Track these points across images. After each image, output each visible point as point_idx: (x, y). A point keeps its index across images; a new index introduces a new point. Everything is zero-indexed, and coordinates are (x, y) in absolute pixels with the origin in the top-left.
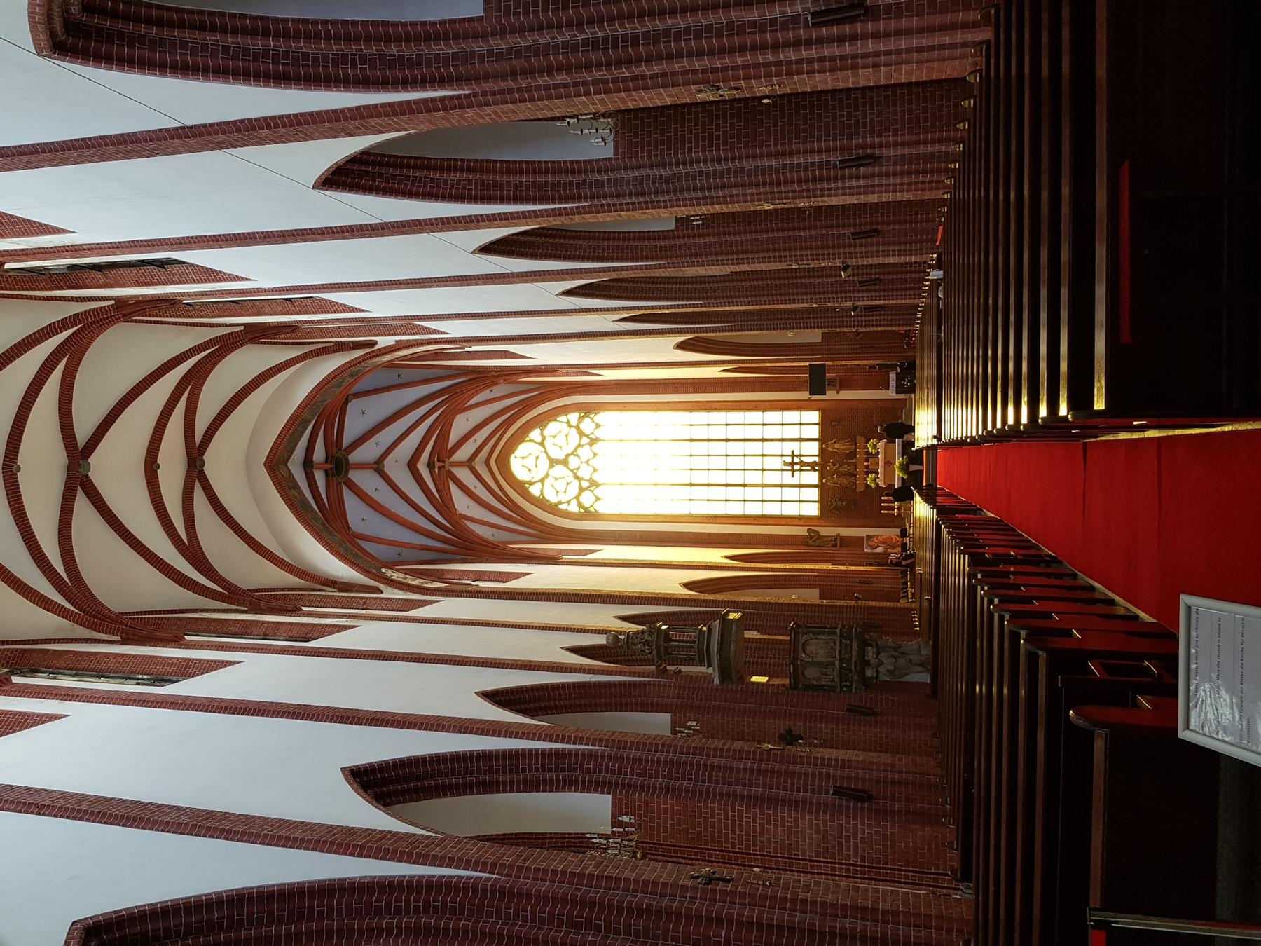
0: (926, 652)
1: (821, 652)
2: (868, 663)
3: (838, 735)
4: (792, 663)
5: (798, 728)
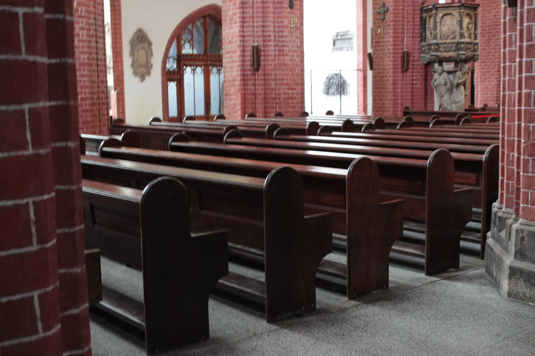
0: (453, 108)
1: (445, 29)
2: (440, 64)
3: (386, 46)
4: (433, 6)
5: (390, 16)
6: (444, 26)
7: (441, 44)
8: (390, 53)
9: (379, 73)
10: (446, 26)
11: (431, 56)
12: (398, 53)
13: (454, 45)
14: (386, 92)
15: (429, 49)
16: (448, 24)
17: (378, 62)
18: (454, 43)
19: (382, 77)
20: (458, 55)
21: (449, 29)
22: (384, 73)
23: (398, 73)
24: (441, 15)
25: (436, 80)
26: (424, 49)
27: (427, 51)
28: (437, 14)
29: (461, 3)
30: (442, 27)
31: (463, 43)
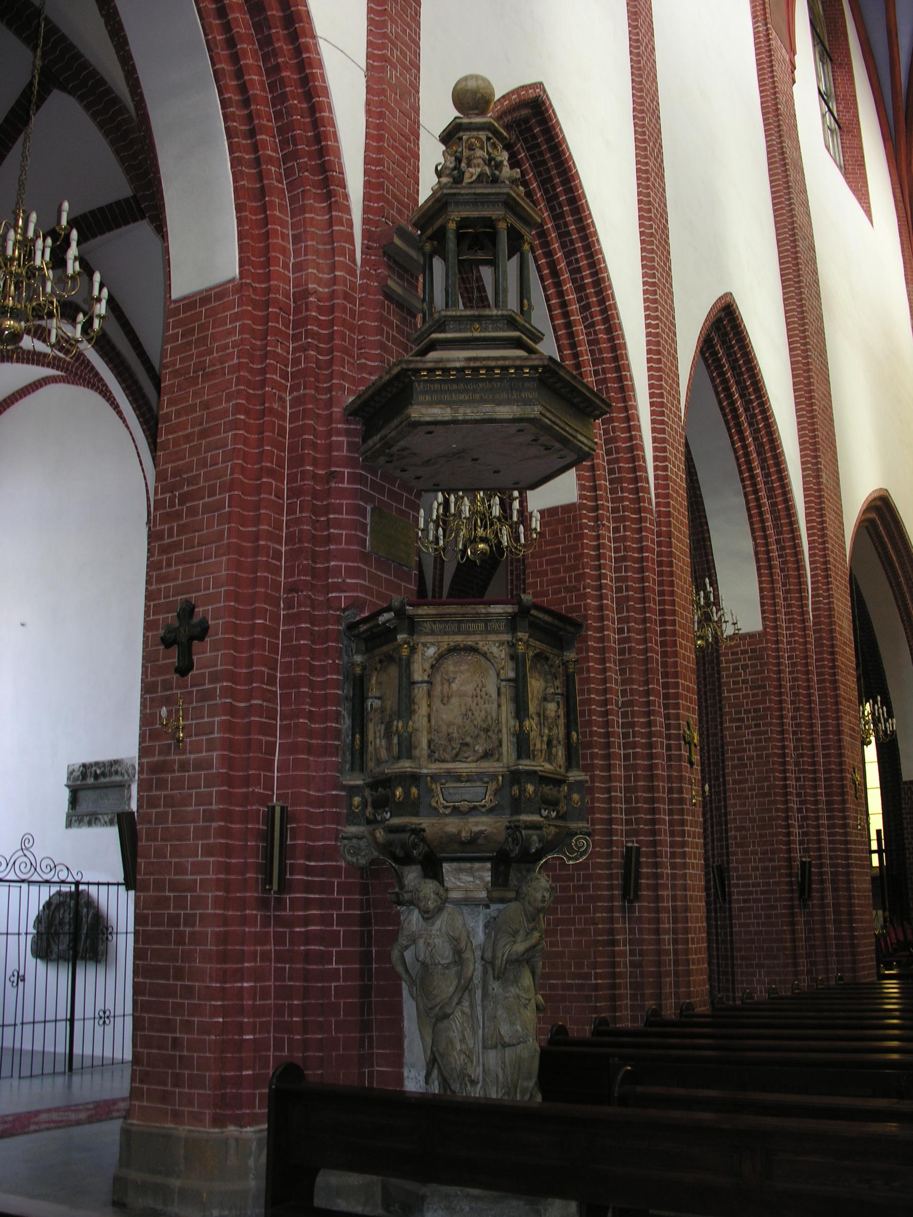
1: (450, 714)
5: (208, 656)
6: (445, 699)
7: (435, 777)
8: (209, 816)
9: (162, 902)
10: (455, 700)
11: (392, 830)
12: (245, 817)
13: (492, 787)
14: (188, 992)
15: (380, 804)
16: (462, 695)
17: (160, 853)
18: (493, 777)
19: (174, 920)
20: (513, 828)
21: (467, 714)
22: (180, 903)
23: (242, 904)
24: (431, 651)
25: (413, 940)
26: (357, 800)
27: (369, 809)
28: (413, 650)
29: (520, 602)
30: (437, 703)
31: (532, 775)
